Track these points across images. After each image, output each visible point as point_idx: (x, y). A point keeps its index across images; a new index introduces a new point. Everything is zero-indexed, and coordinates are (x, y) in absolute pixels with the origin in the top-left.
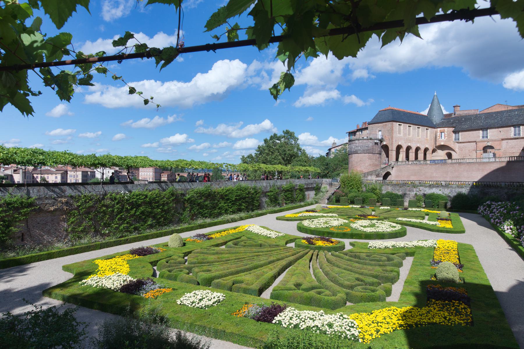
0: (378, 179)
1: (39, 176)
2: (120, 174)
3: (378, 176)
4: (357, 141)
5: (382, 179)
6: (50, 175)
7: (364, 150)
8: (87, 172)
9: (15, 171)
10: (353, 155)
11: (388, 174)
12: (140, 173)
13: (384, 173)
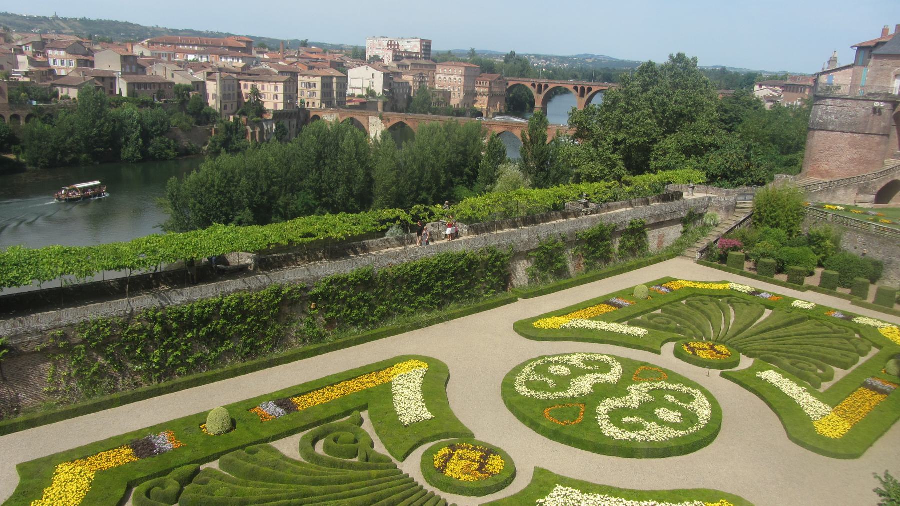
0: (862, 197)
1: (250, 84)
2: (396, 79)
3: (863, 190)
4: (829, 101)
5: (873, 197)
6: (266, 85)
7: (842, 125)
8: (332, 77)
9: (209, 74)
10: (816, 132)
12: (438, 76)
13: (883, 185)
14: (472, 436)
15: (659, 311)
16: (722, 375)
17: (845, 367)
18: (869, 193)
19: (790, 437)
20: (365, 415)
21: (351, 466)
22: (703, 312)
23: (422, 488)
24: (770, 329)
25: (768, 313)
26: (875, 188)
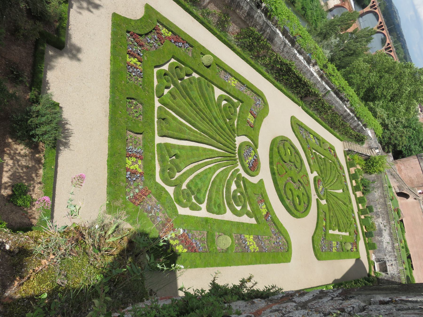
0: (396, 188)
3: (399, 188)
5: (399, 191)
10: (417, 159)
11: (406, 196)
14: (257, 148)
15: (323, 157)
16: (317, 200)
17: (339, 230)
18: (399, 189)
19: (313, 237)
20: (241, 104)
21: (225, 120)
22: (331, 171)
23: (235, 151)
24: (337, 197)
25: (341, 191)
26: (403, 190)
